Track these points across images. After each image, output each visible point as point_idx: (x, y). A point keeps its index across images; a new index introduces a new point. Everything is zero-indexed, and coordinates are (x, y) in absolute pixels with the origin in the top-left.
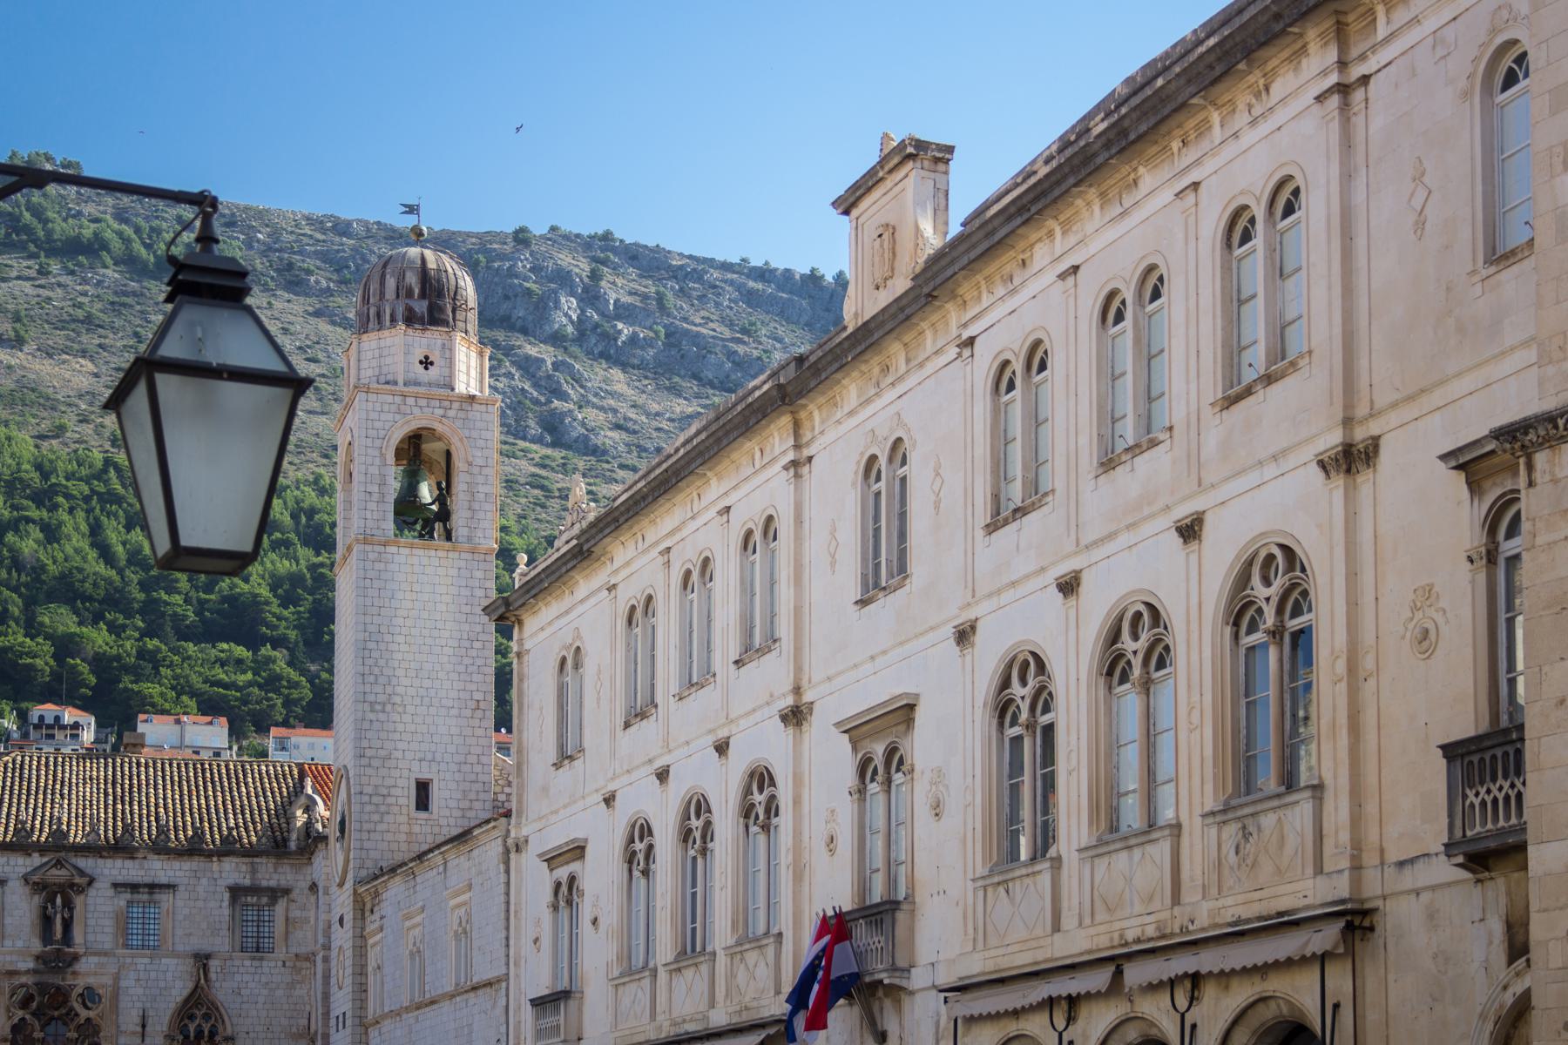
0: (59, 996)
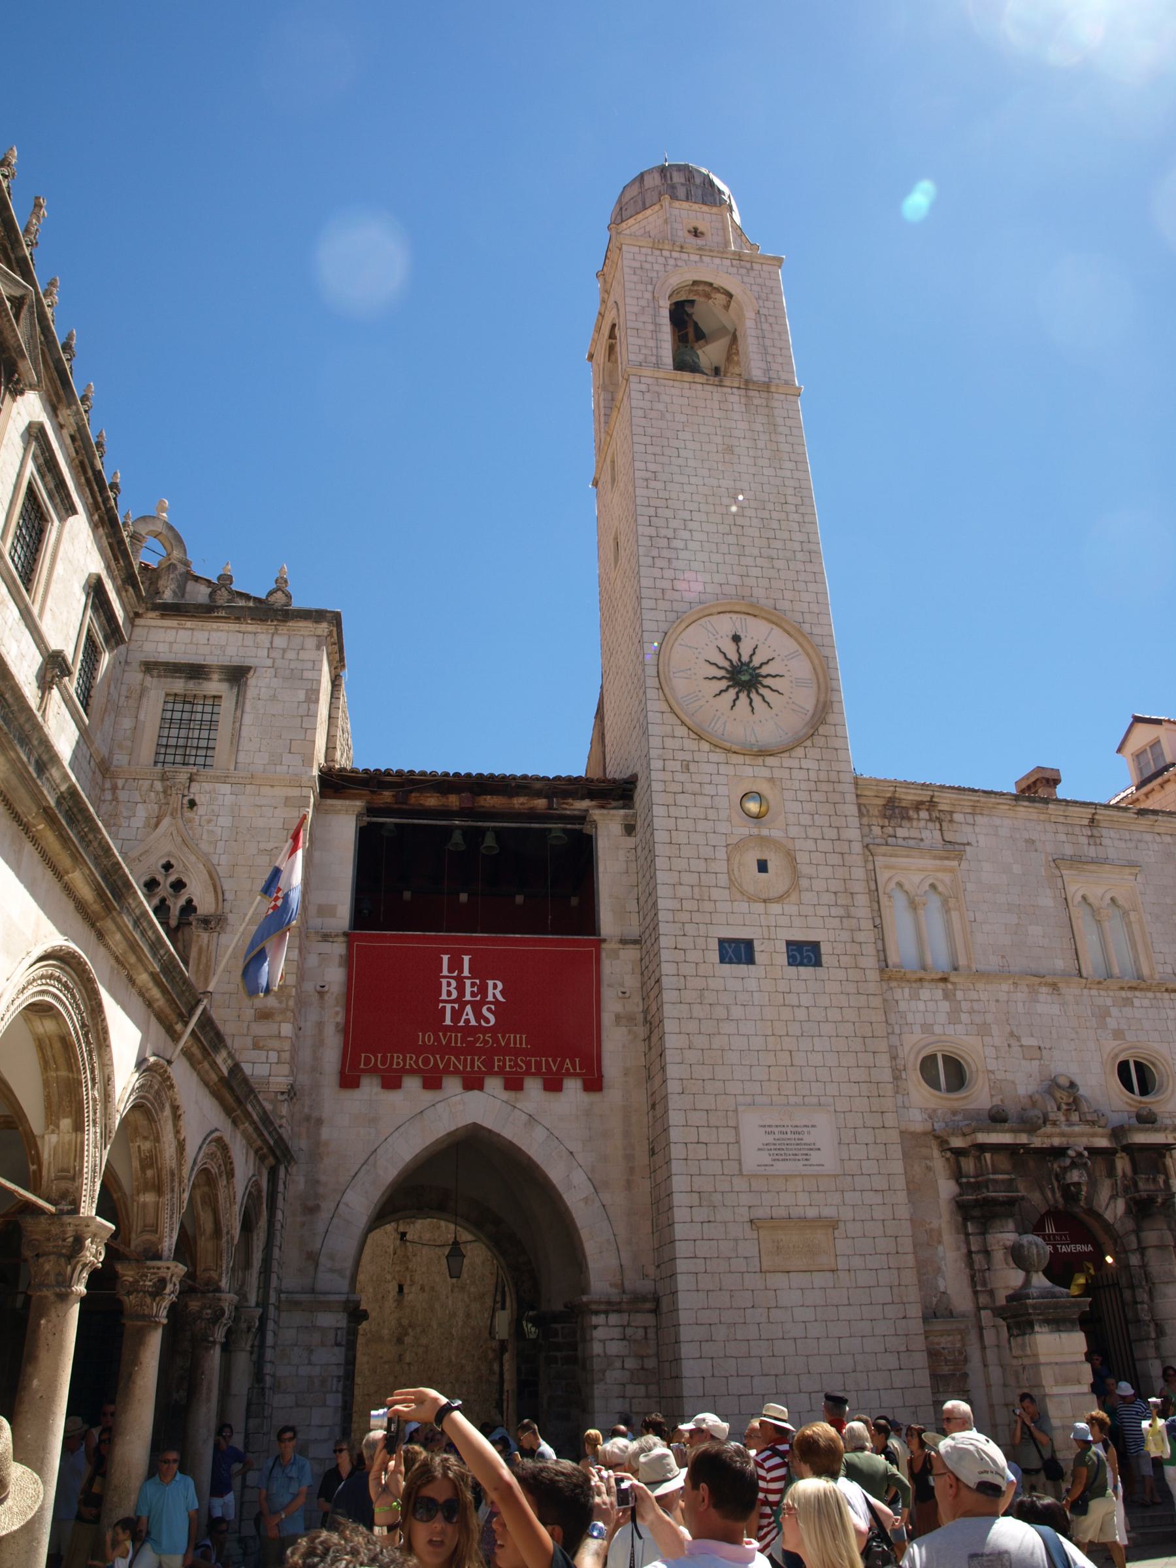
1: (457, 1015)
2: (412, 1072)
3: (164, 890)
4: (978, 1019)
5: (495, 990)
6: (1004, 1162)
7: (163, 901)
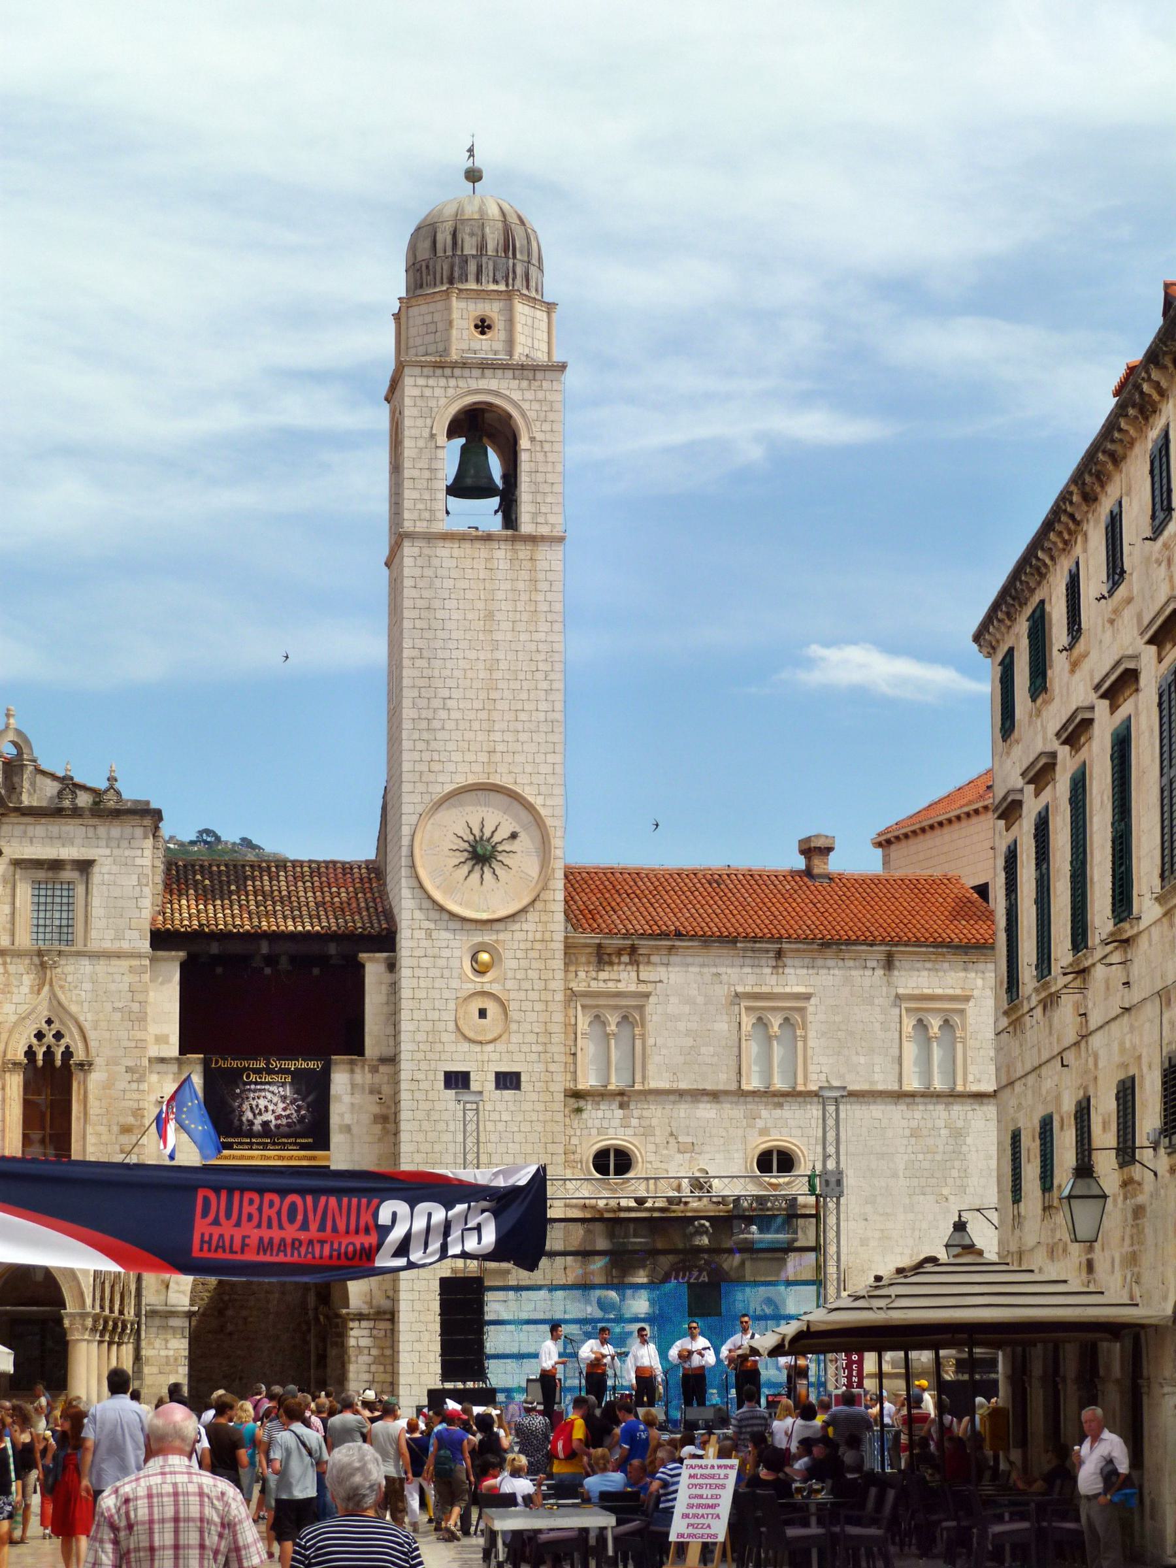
3: (49, 1039)
4: (645, 1123)
7: (49, 1047)
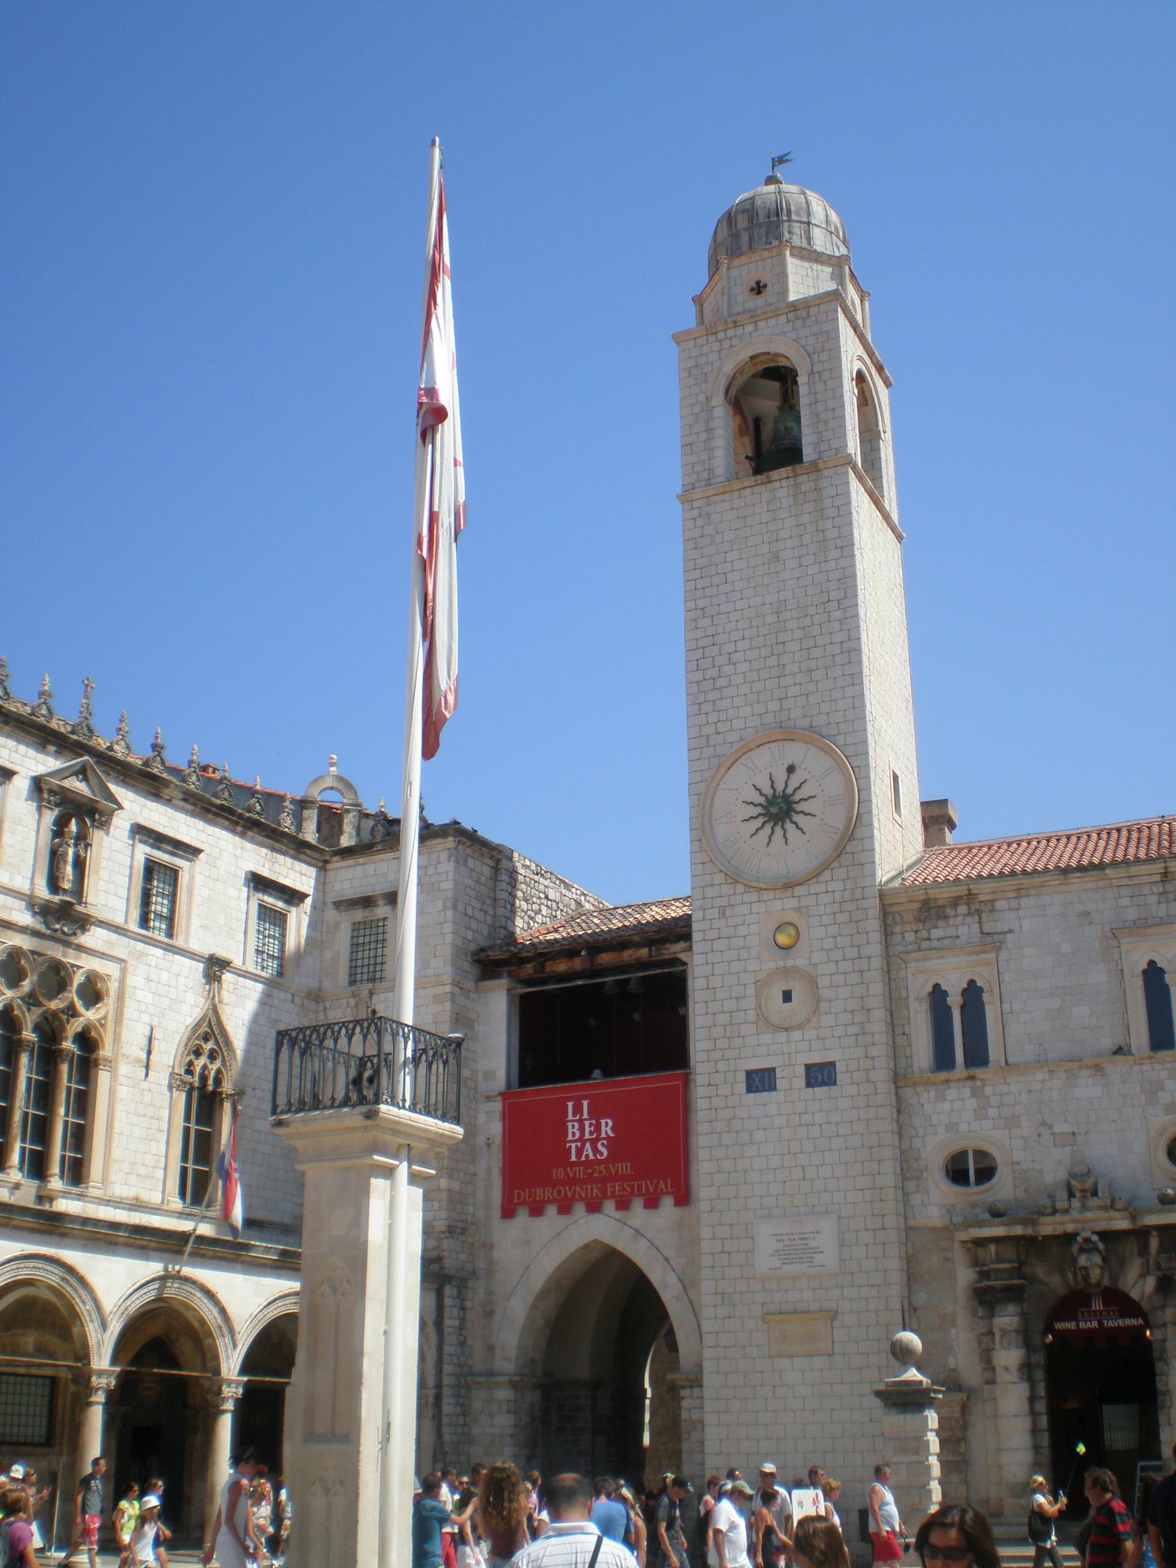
0: (56, 977)
1: (579, 1151)
2: (551, 1201)
5: (607, 1127)
6: (1009, 1252)
